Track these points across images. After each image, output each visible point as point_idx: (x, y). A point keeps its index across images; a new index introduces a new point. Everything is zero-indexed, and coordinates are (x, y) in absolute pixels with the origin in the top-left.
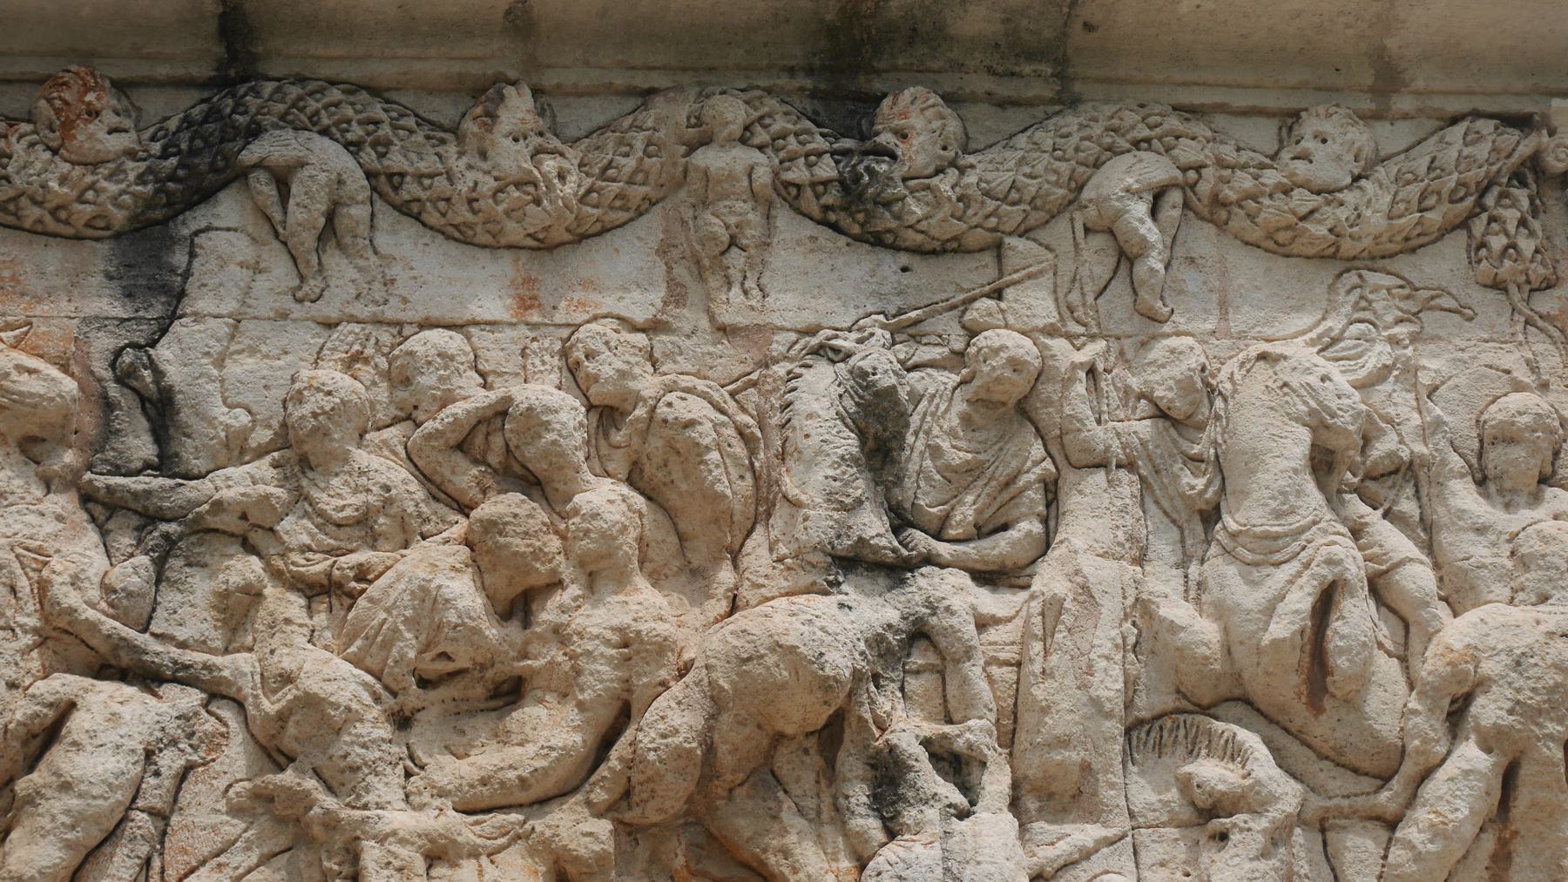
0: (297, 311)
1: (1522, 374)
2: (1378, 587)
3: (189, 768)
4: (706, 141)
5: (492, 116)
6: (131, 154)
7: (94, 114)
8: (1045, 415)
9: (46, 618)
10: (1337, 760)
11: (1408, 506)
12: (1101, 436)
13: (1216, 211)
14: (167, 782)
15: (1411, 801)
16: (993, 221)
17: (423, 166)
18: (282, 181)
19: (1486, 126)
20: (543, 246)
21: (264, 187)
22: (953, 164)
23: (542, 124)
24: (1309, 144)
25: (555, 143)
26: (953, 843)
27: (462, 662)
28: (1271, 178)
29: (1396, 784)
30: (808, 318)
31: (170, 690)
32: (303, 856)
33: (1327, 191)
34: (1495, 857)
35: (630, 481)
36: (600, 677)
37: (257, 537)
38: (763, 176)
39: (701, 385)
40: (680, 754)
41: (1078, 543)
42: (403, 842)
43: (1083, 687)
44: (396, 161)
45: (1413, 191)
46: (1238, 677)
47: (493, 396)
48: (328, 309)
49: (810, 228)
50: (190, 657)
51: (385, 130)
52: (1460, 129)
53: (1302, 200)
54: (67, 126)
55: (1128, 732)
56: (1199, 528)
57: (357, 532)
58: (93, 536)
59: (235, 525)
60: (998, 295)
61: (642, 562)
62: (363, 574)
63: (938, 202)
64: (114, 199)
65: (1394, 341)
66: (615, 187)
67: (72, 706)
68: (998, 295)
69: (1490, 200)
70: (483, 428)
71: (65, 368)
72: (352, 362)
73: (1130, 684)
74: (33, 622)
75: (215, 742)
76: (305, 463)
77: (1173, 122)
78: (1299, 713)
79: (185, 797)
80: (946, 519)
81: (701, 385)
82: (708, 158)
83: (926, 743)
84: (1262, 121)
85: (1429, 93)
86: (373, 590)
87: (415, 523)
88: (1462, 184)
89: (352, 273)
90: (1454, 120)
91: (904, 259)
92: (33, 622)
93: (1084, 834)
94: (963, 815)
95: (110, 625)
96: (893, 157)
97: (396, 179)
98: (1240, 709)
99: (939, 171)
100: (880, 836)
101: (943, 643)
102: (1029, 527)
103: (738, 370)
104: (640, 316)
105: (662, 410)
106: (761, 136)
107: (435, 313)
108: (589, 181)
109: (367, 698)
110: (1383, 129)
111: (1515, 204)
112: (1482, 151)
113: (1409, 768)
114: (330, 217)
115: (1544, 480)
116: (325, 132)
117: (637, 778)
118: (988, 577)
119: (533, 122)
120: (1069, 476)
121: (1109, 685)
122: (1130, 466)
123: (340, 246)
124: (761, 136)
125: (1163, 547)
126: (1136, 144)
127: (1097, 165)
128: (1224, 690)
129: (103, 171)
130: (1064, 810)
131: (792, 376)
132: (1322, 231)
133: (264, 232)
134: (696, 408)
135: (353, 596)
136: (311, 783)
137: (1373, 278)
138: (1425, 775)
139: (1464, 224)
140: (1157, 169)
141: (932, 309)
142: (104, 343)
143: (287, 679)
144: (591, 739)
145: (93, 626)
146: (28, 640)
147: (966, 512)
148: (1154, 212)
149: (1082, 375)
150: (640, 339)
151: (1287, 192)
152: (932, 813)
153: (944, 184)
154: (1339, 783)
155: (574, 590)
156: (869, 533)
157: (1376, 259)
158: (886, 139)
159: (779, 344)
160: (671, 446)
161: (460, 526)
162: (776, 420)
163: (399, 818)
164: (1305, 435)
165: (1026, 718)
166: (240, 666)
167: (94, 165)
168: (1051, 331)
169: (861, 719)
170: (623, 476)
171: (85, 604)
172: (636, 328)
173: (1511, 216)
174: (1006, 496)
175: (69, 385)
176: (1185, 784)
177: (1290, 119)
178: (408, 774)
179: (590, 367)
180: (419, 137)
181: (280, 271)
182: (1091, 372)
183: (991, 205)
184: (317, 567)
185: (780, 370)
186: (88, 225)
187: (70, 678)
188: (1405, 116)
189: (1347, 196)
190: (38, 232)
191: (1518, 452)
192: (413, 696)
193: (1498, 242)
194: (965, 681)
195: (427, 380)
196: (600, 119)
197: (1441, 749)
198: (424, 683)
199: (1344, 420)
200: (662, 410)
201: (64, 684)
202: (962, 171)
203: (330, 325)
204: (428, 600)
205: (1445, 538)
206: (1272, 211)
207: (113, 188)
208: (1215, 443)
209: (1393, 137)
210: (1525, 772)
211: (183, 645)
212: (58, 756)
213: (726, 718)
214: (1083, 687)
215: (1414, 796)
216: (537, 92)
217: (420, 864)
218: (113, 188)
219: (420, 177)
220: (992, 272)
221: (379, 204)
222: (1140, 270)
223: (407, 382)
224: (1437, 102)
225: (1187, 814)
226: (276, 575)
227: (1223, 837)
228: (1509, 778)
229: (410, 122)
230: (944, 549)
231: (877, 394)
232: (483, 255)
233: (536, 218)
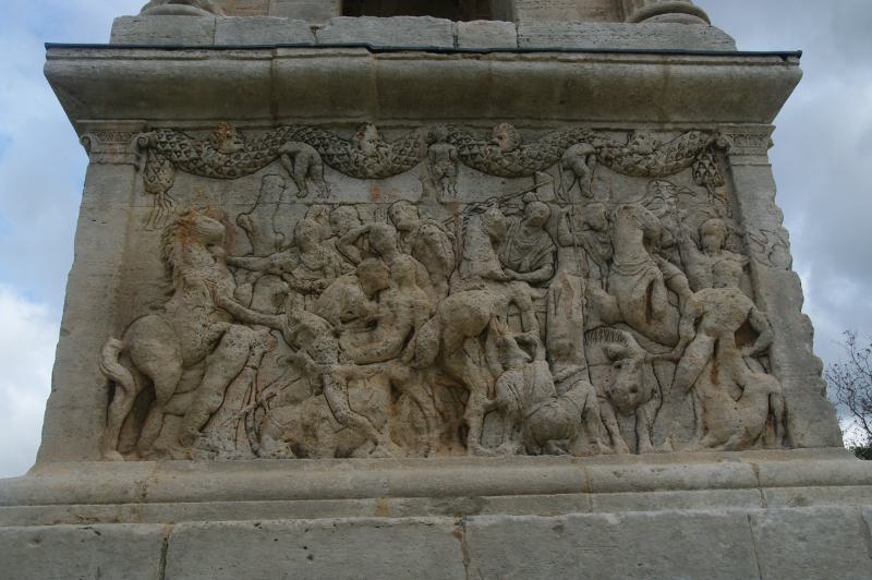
0: (298, 201)
1: (712, 213)
2: (668, 283)
3: (265, 353)
4: (435, 141)
5: (362, 134)
6: (242, 150)
7: (229, 137)
8: (552, 230)
9: (215, 303)
10: (657, 340)
11: (677, 258)
12: (568, 236)
13: (608, 162)
14: (257, 356)
15: (683, 354)
16: (532, 166)
17: (339, 152)
18: (292, 156)
19: (697, 133)
20: (380, 176)
21: (286, 159)
22: (518, 147)
23: (380, 138)
24: (639, 140)
25: (384, 144)
26: (527, 370)
27: (357, 315)
28: (626, 150)
29: (678, 348)
30: (471, 200)
31: (257, 327)
32: (304, 381)
33: (645, 154)
34: (712, 373)
35: (412, 254)
36: (404, 317)
37: (286, 276)
38: (454, 153)
40: (432, 343)
41: (565, 271)
42: (339, 374)
43: (569, 318)
44: (331, 151)
45: (674, 154)
46: (621, 314)
47: (364, 227)
48: (309, 200)
49: (470, 170)
50: (263, 316)
51: (327, 141)
52: (689, 134)
53: (636, 157)
54: (221, 141)
55: (585, 334)
56: (605, 265)
57: (318, 272)
58: (231, 277)
59: (279, 272)
60: (534, 190)
61: (417, 281)
62: (322, 287)
63: (514, 160)
64: (237, 165)
65: (669, 203)
66: (404, 157)
67: (224, 332)
68: (534, 190)
69: (699, 157)
70: (361, 239)
71: (221, 222)
72: (318, 216)
73: (586, 318)
74: (211, 305)
76: (302, 250)
77: (592, 133)
78: (644, 325)
79: (263, 363)
80: (519, 265)
82: (437, 148)
83: (516, 338)
84: (622, 134)
85: (677, 122)
86: (326, 291)
87: (338, 269)
88: (690, 151)
89: (316, 188)
90: (686, 132)
91: (503, 179)
92: (211, 305)
93: (573, 368)
94: (530, 362)
96: (498, 145)
97: (330, 156)
98: (622, 325)
99: (514, 150)
100: (501, 370)
101: (520, 305)
102: (547, 268)
103: (448, 217)
104: (414, 200)
105: (422, 230)
106: (453, 140)
107: (345, 201)
108: (395, 156)
109: (325, 327)
110: (662, 135)
111: (708, 159)
112: (697, 141)
113: (682, 343)
114: (309, 169)
116: (307, 142)
117: (417, 351)
118: (535, 284)
119: (375, 136)
120: (562, 250)
121: (578, 317)
122: (582, 246)
123: (313, 180)
124: (453, 140)
125: (595, 271)
126: (580, 141)
127: (567, 148)
128: (617, 318)
129: (233, 156)
130: (564, 360)
131: (466, 219)
132: (643, 167)
133: (285, 175)
134: (434, 229)
135: (319, 294)
136: (306, 356)
137: (661, 183)
138: (687, 345)
139: (691, 165)
140: (587, 148)
141: (512, 196)
142: (233, 214)
143: (297, 321)
144: (401, 339)
145: (230, 306)
146: (208, 311)
147: (526, 263)
148: (586, 162)
149: (564, 216)
150: (414, 207)
151: (631, 155)
152: (519, 361)
153: (516, 153)
154: (658, 349)
155: (394, 290)
156: (494, 269)
157: (663, 176)
158: (496, 140)
159: (461, 209)
160: (426, 241)
162: (461, 233)
163: (336, 367)
164: (642, 233)
165: (550, 329)
166: (282, 319)
167: (229, 154)
168: (553, 202)
169: (493, 330)
170: (410, 251)
171: (228, 299)
172: (413, 204)
173: (707, 162)
174: (539, 257)
175: (222, 227)
176: (605, 350)
177: (630, 133)
178: (339, 353)
179: (397, 217)
180: (338, 143)
181: (292, 188)
182: (567, 215)
183: (531, 160)
184: (307, 285)
185: (462, 217)
186: (228, 174)
187: (224, 323)
188: (669, 131)
189: (651, 156)
190: (212, 176)
191: (713, 238)
192: (340, 326)
193: (702, 171)
194: (529, 318)
195: (342, 222)
196: (399, 136)
197: (693, 336)
198: (343, 322)
199: (654, 228)
200: (422, 230)
201: (226, 324)
202: (521, 150)
203: (309, 205)
204: (347, 294)
205: (689, 267)
206: (626, 161)
207: (236, 162)
208: (610, 237)
209: (666, 138)
210: (721, 343)
211: (262, 312)
212: (221, 349)
213: (447, 330)
214: (569, 318)
215: (684, 351)
216: (378, 128)
217: (344, 382)
218: (236, 162)
219: (338, 156)
220: (532, 184)
221: (325, 166)
222: (583, 181)
223: (336, 223)
224: (680, 126)
225: (606, 360)
226: (293, 288)
227: (619, 367)
228: (716, 345)
229: (335, 138)
230: (518, 275)
231: (496, 222)
232: (361, 181)
233: (378, 167)
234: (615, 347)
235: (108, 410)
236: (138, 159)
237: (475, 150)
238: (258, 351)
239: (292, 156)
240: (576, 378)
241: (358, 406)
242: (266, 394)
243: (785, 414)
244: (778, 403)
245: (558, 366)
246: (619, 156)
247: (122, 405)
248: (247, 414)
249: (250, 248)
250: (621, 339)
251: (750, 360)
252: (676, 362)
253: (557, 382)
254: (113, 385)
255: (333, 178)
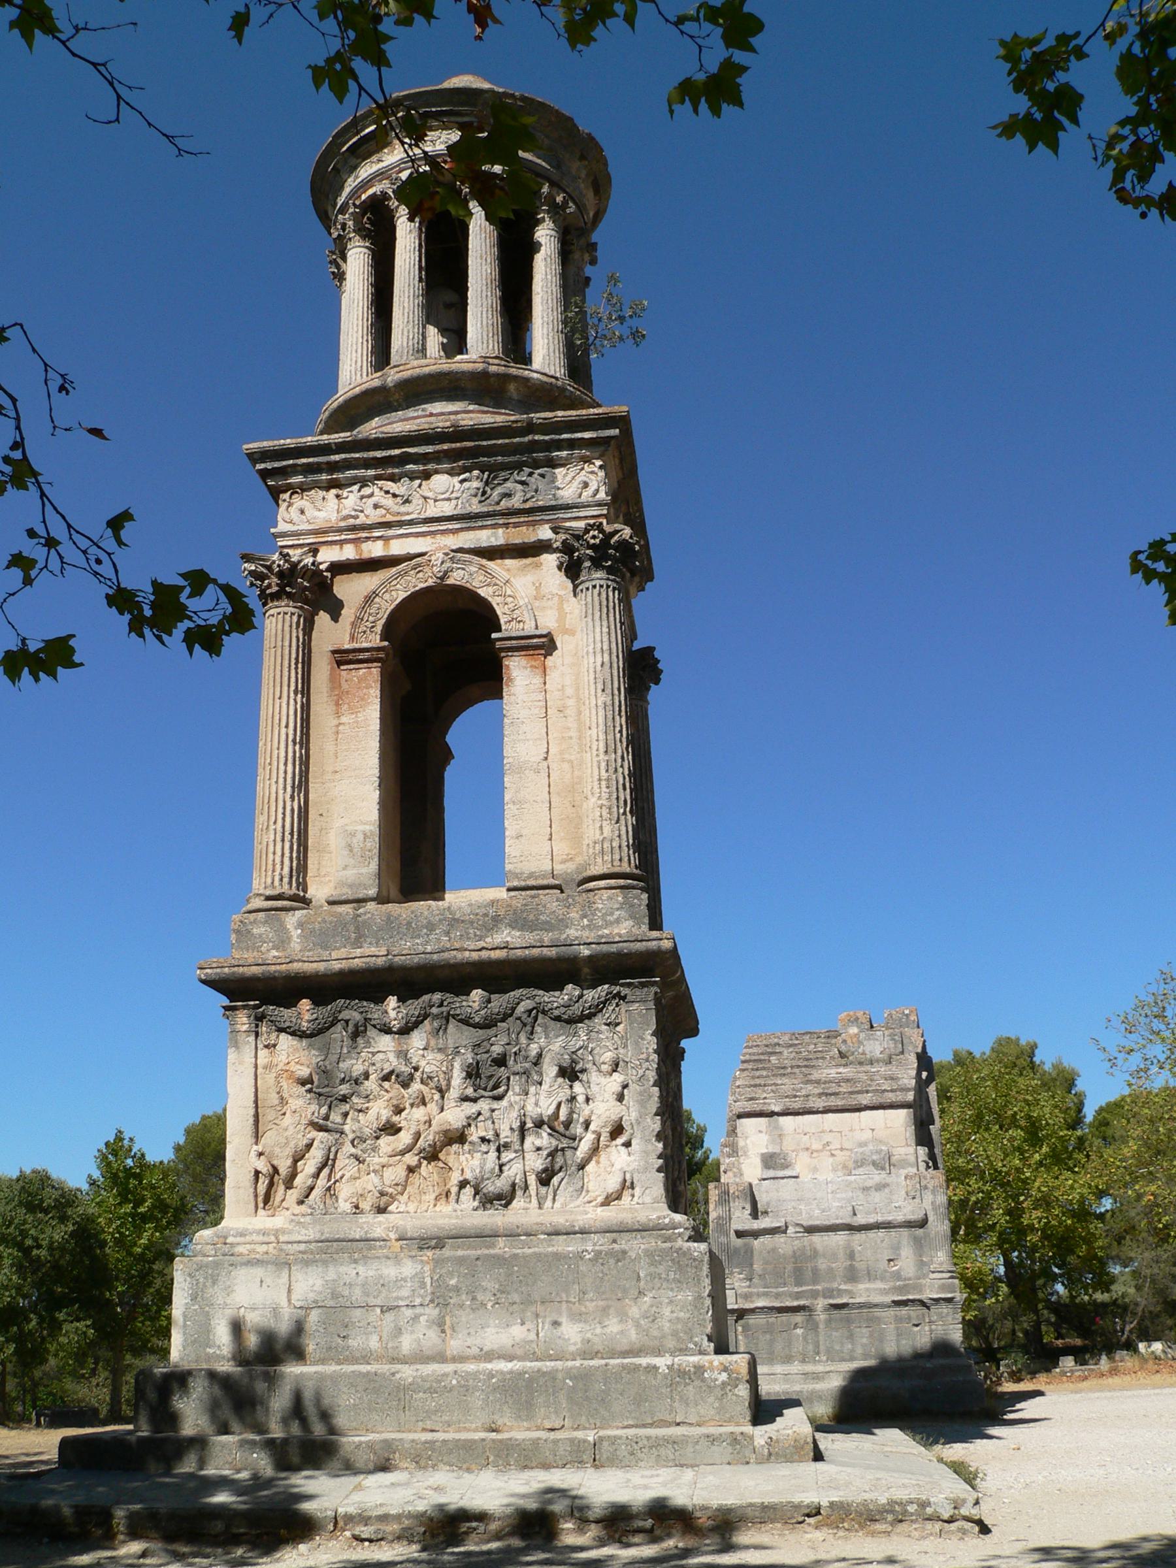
28: (555, 1005)
39: (434, 1062)
44: (369, 1016)
50: (336, 1126)
53: (563, 1010)
60: (496, 1036)
62: (367, 1108)
68: (496, 1036)
75: (342, 1144)
81: (434, 1062)
86: (370, 1112)
95: (321, 1121)
97: (370, 1019)
112: (604, 994)
115: (615, 1071)
122: (525, 1073)
124: (445, 1003)
127: (518, 1003)
148: (529, 1016)
153: (483, 1012)
161: (387, 1096)
164: (557, 1068)
168: (508, 1044)
173: (611, 1008)
185: (450, 1057)
193: (607, 1015)
206: (556, 1013)
230: (486, 1094)
234: (538, 1143)
235: (256, 1188)
236: (257, 1026)
237: (458, 1012)
238: (333, 1149)
239: (347, 1022)
240: (514, 1161)
241: (387, 1182)
242: (340, 1174)
243: (632, 1183)
244: (628, 1177)
245: (503, 1155)
246: (552, 1009)
247: (262, 1187)
248: (330, 1187)
249: (326, 1082)
250: (542, 1138)
251: (619, 1147)
252: (576, 1149)
253: (501, 1166)
254: (257, 1173)
255: (372, 1032)
